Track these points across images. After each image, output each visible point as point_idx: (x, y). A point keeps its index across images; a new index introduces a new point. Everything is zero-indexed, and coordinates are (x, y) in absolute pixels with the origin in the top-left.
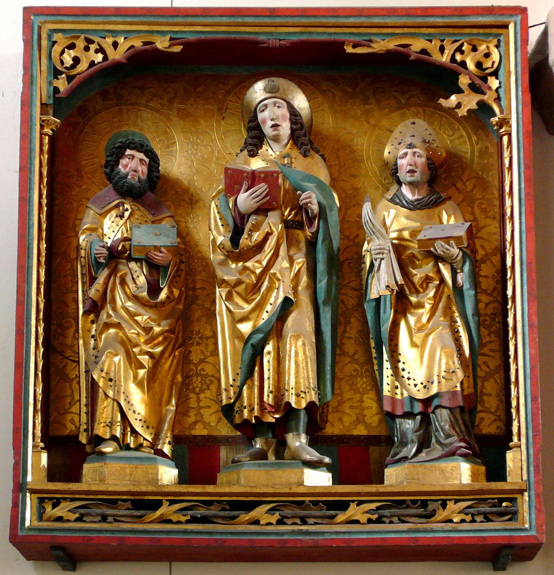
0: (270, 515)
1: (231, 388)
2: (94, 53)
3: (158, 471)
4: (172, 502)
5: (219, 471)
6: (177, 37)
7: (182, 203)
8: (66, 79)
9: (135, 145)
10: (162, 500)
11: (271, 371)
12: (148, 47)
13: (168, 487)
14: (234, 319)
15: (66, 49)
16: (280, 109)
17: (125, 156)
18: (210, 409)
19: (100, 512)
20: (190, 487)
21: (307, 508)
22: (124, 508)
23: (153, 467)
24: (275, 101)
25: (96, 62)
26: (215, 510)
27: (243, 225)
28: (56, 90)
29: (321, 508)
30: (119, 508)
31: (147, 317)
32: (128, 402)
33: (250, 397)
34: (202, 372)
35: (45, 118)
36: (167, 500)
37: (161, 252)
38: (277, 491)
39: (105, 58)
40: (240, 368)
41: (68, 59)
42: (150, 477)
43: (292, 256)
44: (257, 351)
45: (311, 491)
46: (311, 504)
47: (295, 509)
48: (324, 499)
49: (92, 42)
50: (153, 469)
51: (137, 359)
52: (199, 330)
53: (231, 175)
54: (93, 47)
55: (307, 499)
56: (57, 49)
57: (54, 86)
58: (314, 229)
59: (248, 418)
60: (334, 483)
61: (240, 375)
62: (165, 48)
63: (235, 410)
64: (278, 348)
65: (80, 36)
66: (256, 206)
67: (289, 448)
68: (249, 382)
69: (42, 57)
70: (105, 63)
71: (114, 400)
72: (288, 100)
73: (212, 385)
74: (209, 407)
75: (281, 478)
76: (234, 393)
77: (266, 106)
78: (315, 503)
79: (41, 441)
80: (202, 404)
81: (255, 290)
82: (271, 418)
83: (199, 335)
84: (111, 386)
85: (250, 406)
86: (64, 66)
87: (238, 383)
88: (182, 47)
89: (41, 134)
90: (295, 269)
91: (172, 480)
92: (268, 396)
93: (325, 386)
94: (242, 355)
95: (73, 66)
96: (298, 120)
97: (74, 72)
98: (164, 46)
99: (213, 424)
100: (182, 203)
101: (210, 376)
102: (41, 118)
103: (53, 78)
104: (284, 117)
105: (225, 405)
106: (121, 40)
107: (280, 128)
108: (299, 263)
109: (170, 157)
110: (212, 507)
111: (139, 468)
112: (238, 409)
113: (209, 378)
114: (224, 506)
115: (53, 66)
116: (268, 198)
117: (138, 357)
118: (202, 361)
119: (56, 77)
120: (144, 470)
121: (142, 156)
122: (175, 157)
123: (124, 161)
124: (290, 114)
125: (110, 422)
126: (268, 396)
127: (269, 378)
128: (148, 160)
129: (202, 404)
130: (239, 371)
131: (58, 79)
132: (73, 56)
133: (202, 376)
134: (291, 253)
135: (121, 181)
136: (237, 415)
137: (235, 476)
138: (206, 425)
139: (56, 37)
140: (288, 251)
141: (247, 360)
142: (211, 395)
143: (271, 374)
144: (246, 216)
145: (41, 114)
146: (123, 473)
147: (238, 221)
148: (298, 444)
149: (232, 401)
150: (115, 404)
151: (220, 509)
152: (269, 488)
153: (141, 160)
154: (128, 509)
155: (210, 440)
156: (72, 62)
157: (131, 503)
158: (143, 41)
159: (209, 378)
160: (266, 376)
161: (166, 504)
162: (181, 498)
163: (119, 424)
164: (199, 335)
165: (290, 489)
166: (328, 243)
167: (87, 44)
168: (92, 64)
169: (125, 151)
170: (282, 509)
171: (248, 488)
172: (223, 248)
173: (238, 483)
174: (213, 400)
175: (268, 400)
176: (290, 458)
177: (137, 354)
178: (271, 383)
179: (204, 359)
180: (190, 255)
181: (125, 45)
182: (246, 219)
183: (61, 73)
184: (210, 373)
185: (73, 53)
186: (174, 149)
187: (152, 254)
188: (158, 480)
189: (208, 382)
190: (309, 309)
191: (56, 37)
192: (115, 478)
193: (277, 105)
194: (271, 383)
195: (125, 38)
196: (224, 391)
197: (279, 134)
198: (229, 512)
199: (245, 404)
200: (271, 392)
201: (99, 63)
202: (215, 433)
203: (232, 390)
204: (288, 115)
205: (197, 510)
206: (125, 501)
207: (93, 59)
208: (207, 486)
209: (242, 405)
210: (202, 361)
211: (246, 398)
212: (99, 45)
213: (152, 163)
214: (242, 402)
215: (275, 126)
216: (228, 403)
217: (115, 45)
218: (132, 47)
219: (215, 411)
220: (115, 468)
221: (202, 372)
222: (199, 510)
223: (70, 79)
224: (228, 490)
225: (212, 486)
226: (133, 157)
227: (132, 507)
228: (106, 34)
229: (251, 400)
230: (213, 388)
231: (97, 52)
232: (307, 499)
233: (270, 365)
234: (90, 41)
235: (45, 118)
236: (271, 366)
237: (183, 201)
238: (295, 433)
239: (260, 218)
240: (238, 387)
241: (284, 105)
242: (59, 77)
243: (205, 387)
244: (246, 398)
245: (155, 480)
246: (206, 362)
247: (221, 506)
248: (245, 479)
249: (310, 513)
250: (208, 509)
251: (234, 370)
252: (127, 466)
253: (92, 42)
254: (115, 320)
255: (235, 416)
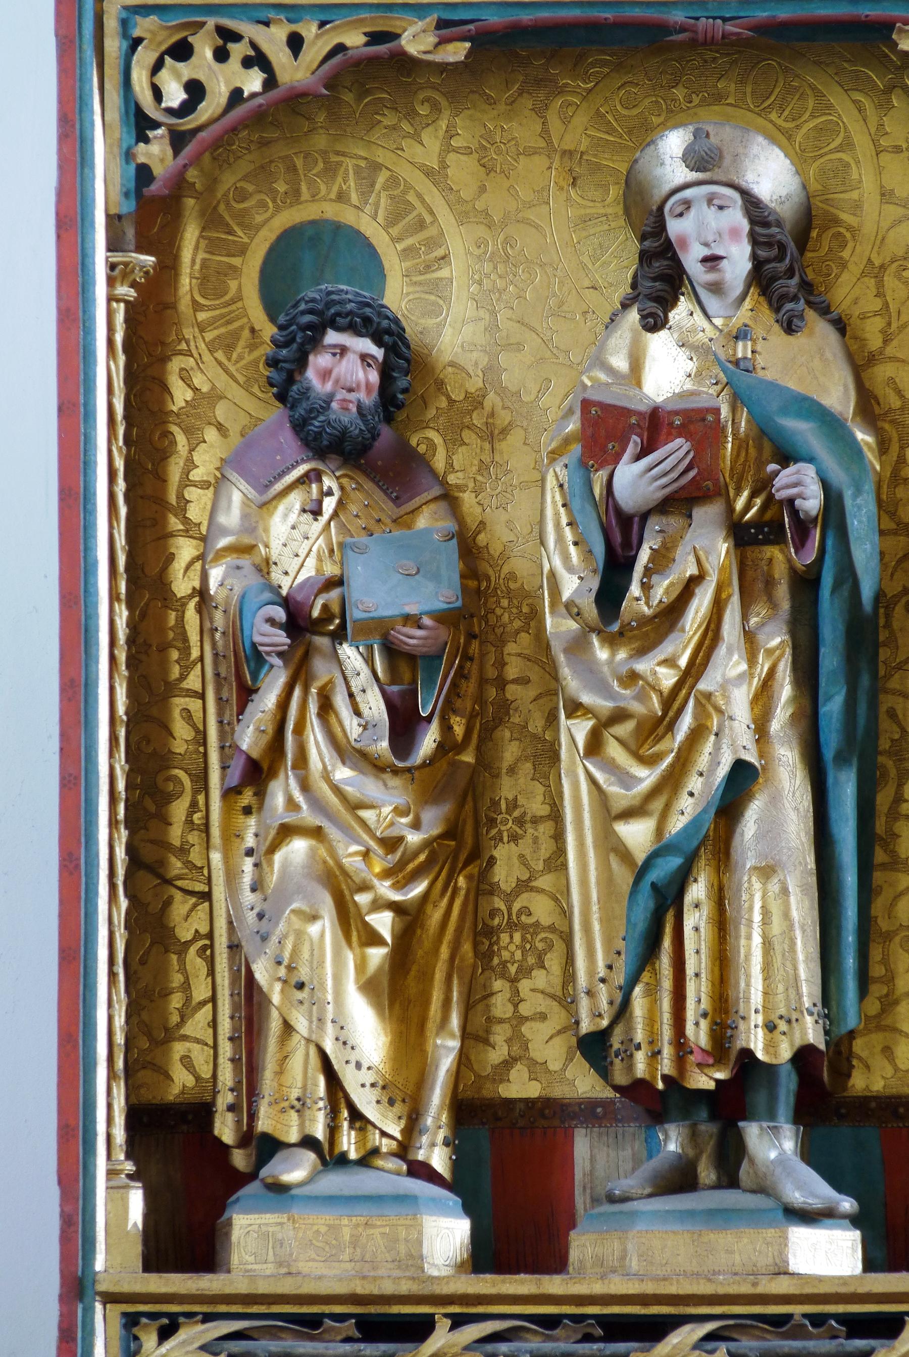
0: (704, 1354)
1: (602, 985)
2: (240, 65)
3: (420, 1233)
4: (458, 1321)
5: (573, 1225)
6: (456, 17)
7: (467, 435)
8: (167, 141)
9: (349, 318)
10: (433, 1315)
11: (703, 957)
12: (382, 49)
13: (448, 1283)
14: (608, 811)
15: (166, 57)
16: (726, 212)
17: (324, 346)
18: (547, 1023)
19: (279, 1349)
20: (503, 1282)
21: (798, 1333)
22: (339, 1338)
23: (408, 1222)
24: (713, 193)
25: (246, 94)
26: (566, 1339)
27: (631, 547)
28: (144, 174)
29: (835, 1333)
30: (326, 1336)
31: (391, 808)
32: (345, 1043)
33: (651, 1020)
34: (523, 918)
35: (117, 258)
36: (446, 1315)
37: (420, 627)
38: (721, 1291)
39: (270, 83)
40: (624, 939)
41: (175, 95)
42: (402, 1248)
43: (755, 634)
44: (667, 899)
45: (808, 1290)
46: (808, 1323)
47: (768, 1336)
48: (840, 1309)
49: (236, 37)
50: (408, 1227)
51: (366, 925)
52: (516, 799)
53: (598, 416)
54: (238, 50)
55: (797, 1310)
56: (144, 57)
57: (139, 161)
58: (810, 556)
59: (647, 1077)
60: (869, 1265)
61: (623, 956)
62: (425, 53)
63: (611, 1046)
64: (721, 889)
65: (204, 23)
66: (661, 494)
67: (752, 1162)
68: (646, 976)
69: (107, 86)
70: (274, 94)
71: (308, 1041)
72: (743, 184)
73: (548, 955)
74: (543, 1017)
75: (733, 1252)
76: (611, 1003)
77: (687, 204)
78: (818, 1320)
79: (128, 1156)
80: (525, 1009)
81: (661, 729)
82: (704, 1078)
83: (516, 814)
84: (301, 1002)
85: (651, 1043)
86: (163, 105)
87: (620, 978)
88: (468, 45)
89: (111, 299)
90: (762, 670)
91: (455, 1244)
92: (697, 1024)
93: (841, 990)
94: (630, 909)
95: (187, 108)
96: (772, 236)
97: (189, 123)
98: (422, 48)
99: (555, 1066)
100: (467, 435)
101: (544, 929)
102: (107, 258)
103: (133, 141)
104: (734, 233)
105: (587, 1034)
106: (309, 30)
107: (725, 262)
108: (769, 652)
109: (433, 298)
110: (557, 1332)
111: (374, 1226)
112: (619, 1046)
113: (543, 935)
114: (589, 1330)
115: (133, 106)
116: (692, 474)
117: (367, 918)
118: (524, 886)
119: (142, 138)
120: (387, 1230)
121: (367, 345)
122: (448, 300)
123: (319, 361)
124: (752, 222)
125: (298, 1099)
126: (697, 1024)
127: (697, 975)
128: (382, 351)
129: (525, 1009)
130: (621, 945)
131: (147, 140)
132: (185, 79)
133: (524, 928)
134: (754, 621)
135: (315, 418)
136: (617, 1061)
137: (616, 1244)
138: (536, 1069)
139: (143, 26)
140: (745, 617)
141: (641, 924)
142: (548, 982)
143: (703, 965)
144: (636, 519)
145: (110, 249)
146: (334, 1242)
147: (618, 538)
148: (773, 1155)
149: (605, 1023)
150: (313, 1051)
151: (579, 1336)
152: (702, 1281)
153: (364, 358)
154: (348, 1340)
155: (547, 1111)
156: (183, 96)
157: (356, 1323)
158: (367, 30)
159: (543, 935)
160: (690, 969)
161: (443, 1325)
162: (481, 1309)
163: (321, 1104)
164: (516, 814)
165: (755, 1284)
166: (846, 594)
167: (220, 42)
168: (236, 96)
169: (323, 333)
170: (735, 1336)
171: (650, 1283)
172: (578, 614)
173: (623, 1266)
174: (553, 997)
175: (697, 1034)
176: (754, 1187)
177: (364, 911)
178: (703, 989)
179: (530, 879)
180: (488, 587)
181: (320, 43)
182: (636, 527)
183: (156, 125)
184: (546, 921)
185: (186, 70)
186: (444, 273)
187: (399, 633)
188: (421, 1257)
189: (540, 946)
190: (798, 782)
191: (143, 26)
192: (314, 1256)
193: (716, 202)
194: (703, 989)
195: (322, 24)
196: (583, 995)
197: (723, 279)
198: (601, 1345)
199: (640, 1035)
200: (705, 1015)
201: (254, 95)
202: (558, 1092)
203: (603, 993)
204: (745, 225)
205: (520, 1339)
206: (340, 1318)
207: (238, 85)
208: (546, 1278)
209: (631, 1040)
210: (524, 886)
211: (640, 1020)
212: (253, 45)
213: (392, 356)
214: (630, 1029)
215: (712, 261)
216: (592, 1028)
217: (295, 43)
218: (340, 48)
219: (558, 1028)
220: (315, 1228)
221: (523, 918)
222: (526, 1340)
223: (178, 140)
224: (598, 1288)
225: (557, 1278)
226: (343, 350)
227: (358, 1335)
228: (272, 15)
229: (653, 1026)
230: (554, 961)
231: (247, 63)
232: (797, 1310)
233: (700, 937)
234: (228, 35)
235: (117, 258)
236: (703, 943)
237: (468, 427)
238: (765, 1124)
239: (674, 522)
240: (621, 988)
241: (735, 202)
242: (151, 134)
243: (531, 960)
244: (640, 1020)
245: (416, 1259)
246: (532, 889)
247: (582, 1328)
248: (640, 1256)
249: (804, 1348)
250: (549, 1338)
251: (608, 941)
252: (345, 1221)
253: (236, 37)
254: (307, 816)
255: (612, 1063)
